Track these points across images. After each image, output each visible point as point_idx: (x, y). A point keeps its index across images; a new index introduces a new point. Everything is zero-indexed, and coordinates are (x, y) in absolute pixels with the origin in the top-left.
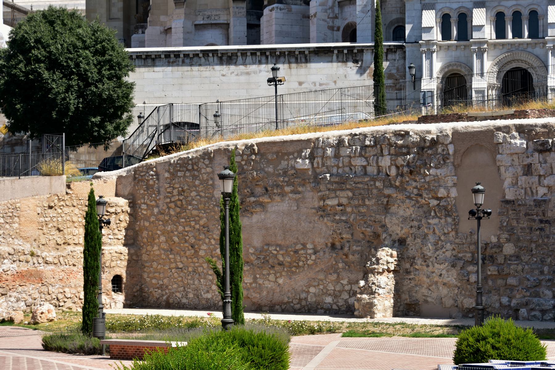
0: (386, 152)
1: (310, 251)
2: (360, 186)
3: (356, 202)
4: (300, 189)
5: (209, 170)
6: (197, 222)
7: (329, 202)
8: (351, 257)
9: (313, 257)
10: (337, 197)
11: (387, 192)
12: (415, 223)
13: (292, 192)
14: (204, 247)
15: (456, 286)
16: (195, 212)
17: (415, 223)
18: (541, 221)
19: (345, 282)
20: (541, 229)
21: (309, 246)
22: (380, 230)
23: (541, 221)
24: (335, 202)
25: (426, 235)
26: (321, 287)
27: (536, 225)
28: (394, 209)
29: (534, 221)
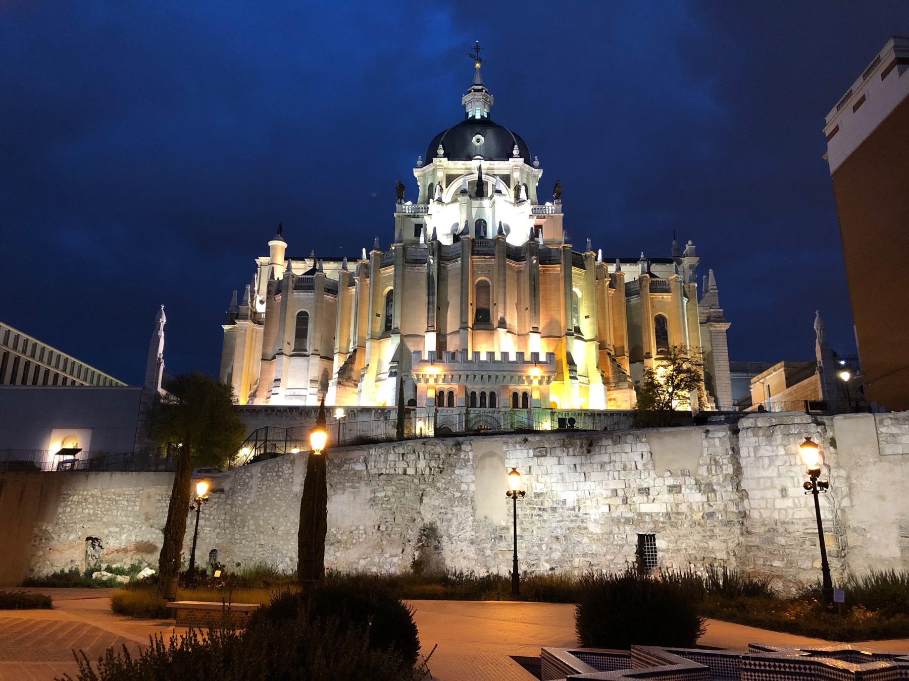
6: (278, 510)
8: (392, 536)
9: (364, 536)
11: (422, 487)
13: (351, 487)
14: (282, 528)
18: (540, 509)
20: (539, 515)
21: (362, 528)
22: (416, 516)
23: (540, 509)
25: (450, 520)
27: (535, 512)
28: (426, 500)
29: (534, 509)
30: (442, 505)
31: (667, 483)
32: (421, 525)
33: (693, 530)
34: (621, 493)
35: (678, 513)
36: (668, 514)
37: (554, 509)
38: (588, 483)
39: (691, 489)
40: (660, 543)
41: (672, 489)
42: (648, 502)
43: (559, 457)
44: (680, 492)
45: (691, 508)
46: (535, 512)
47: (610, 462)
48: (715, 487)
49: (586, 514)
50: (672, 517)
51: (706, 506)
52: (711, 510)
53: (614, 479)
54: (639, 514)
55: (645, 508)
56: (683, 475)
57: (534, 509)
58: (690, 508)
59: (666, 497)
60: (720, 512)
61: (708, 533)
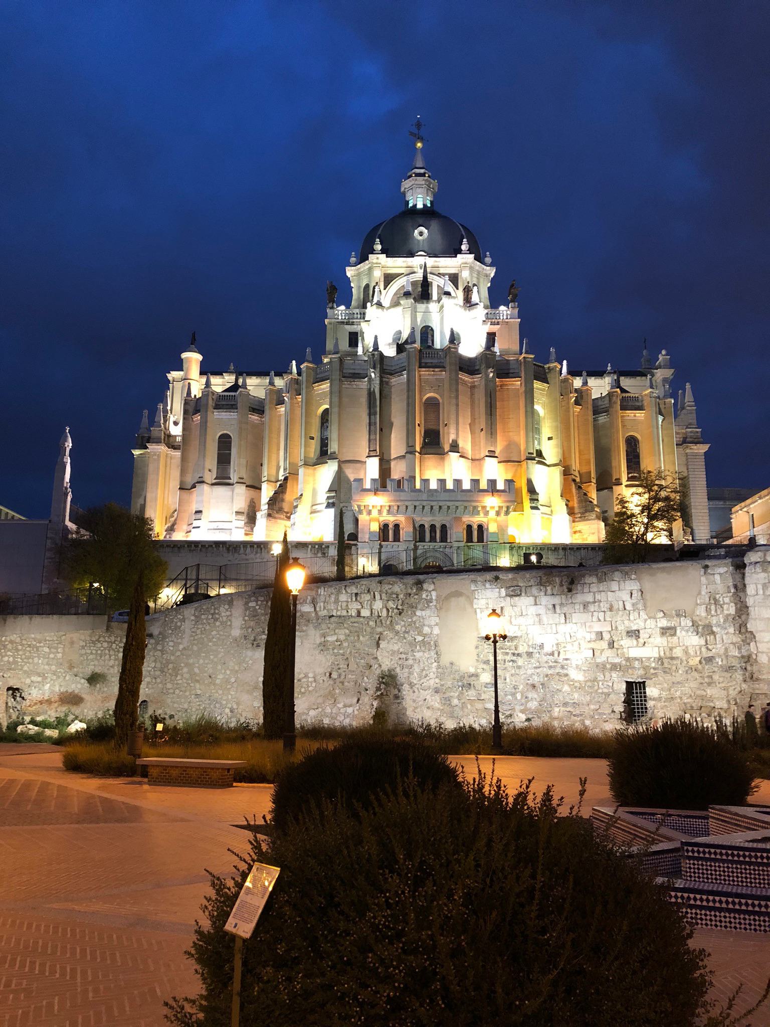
0: (378, 596)
1: (310, 680)
2: (356, 625)
3: (352, 638)
4: (304, 628)
5: (228, 613)
7: (329, 639)
8: (346, 684)
9: (314, 684)
10: (335, 634)
11: (379, 630)
12: (403, 656)
14: (220, 676)
15: (439, 709)
16: (214, 648)
17: (403, 656)
18: (514, 654)
19: (340, 706)
21: (311, 675)
22: (372, 662)
23: (514, 654)
24: (334, 638)
25: (411, 667)
26: (320, 710)
27: (508, 658)
28: (383, 644)
30: (401, 650)
31: (660, 625)
32: (378, 672)
33: (689, 676)
34: (606, 636)
35: (672, 658)
36: (660, 659)
37: (530, 654)
38: (569, 626)
39: (687, 631)
40: (651, 691)
41: (664, 631)
42: (637, 646)
43: (536, 597)
44: (675, 634)
45: (686, 652)
46: (508, 658)
47: (595, 602)
48: (714, 629)
49: (567, 659)
50: (665, 662)
51: (704, 649)
52: (710, 654)
53: (599, 620)
54: (628, 659)
55: (635, 652)
56: (678, 615)
57: (507, 654)
58: (686, 652)
59: (659, 640)
60: (720, 656)
61: (706, 680)
